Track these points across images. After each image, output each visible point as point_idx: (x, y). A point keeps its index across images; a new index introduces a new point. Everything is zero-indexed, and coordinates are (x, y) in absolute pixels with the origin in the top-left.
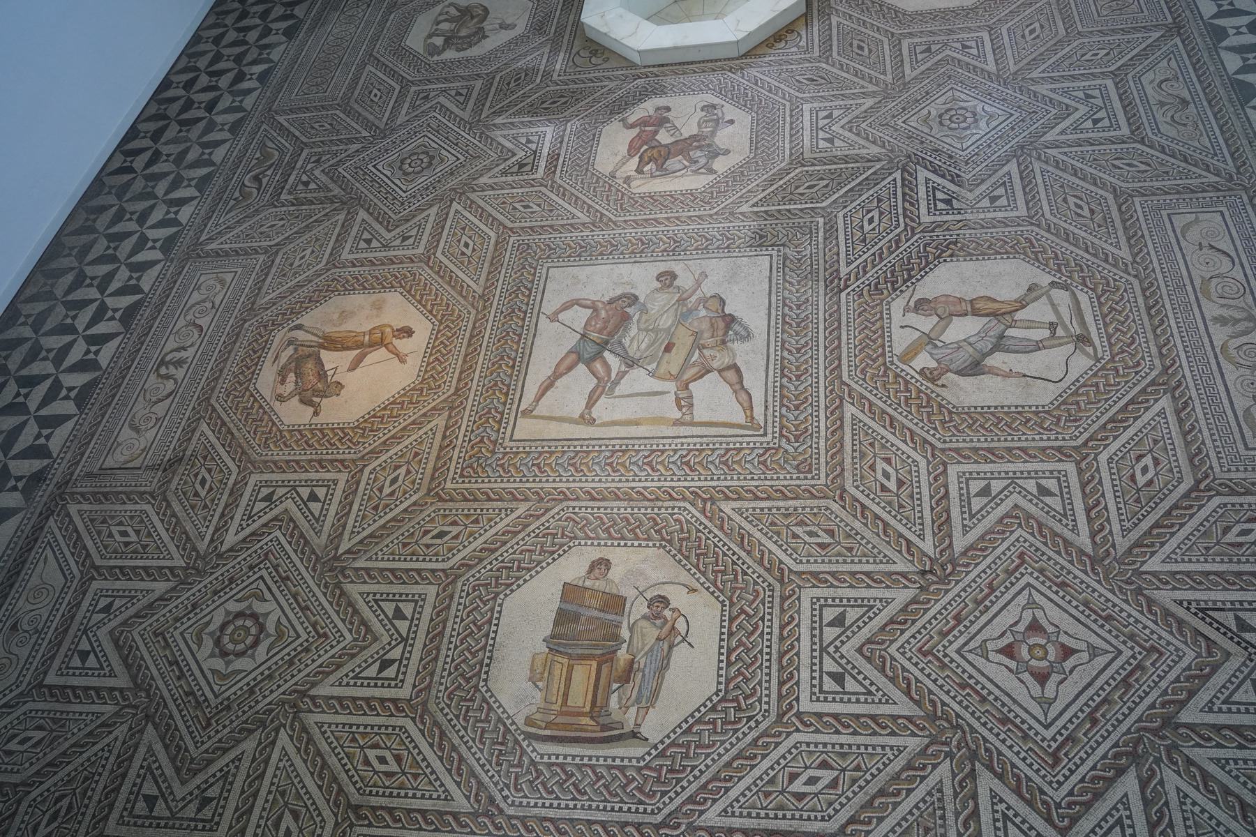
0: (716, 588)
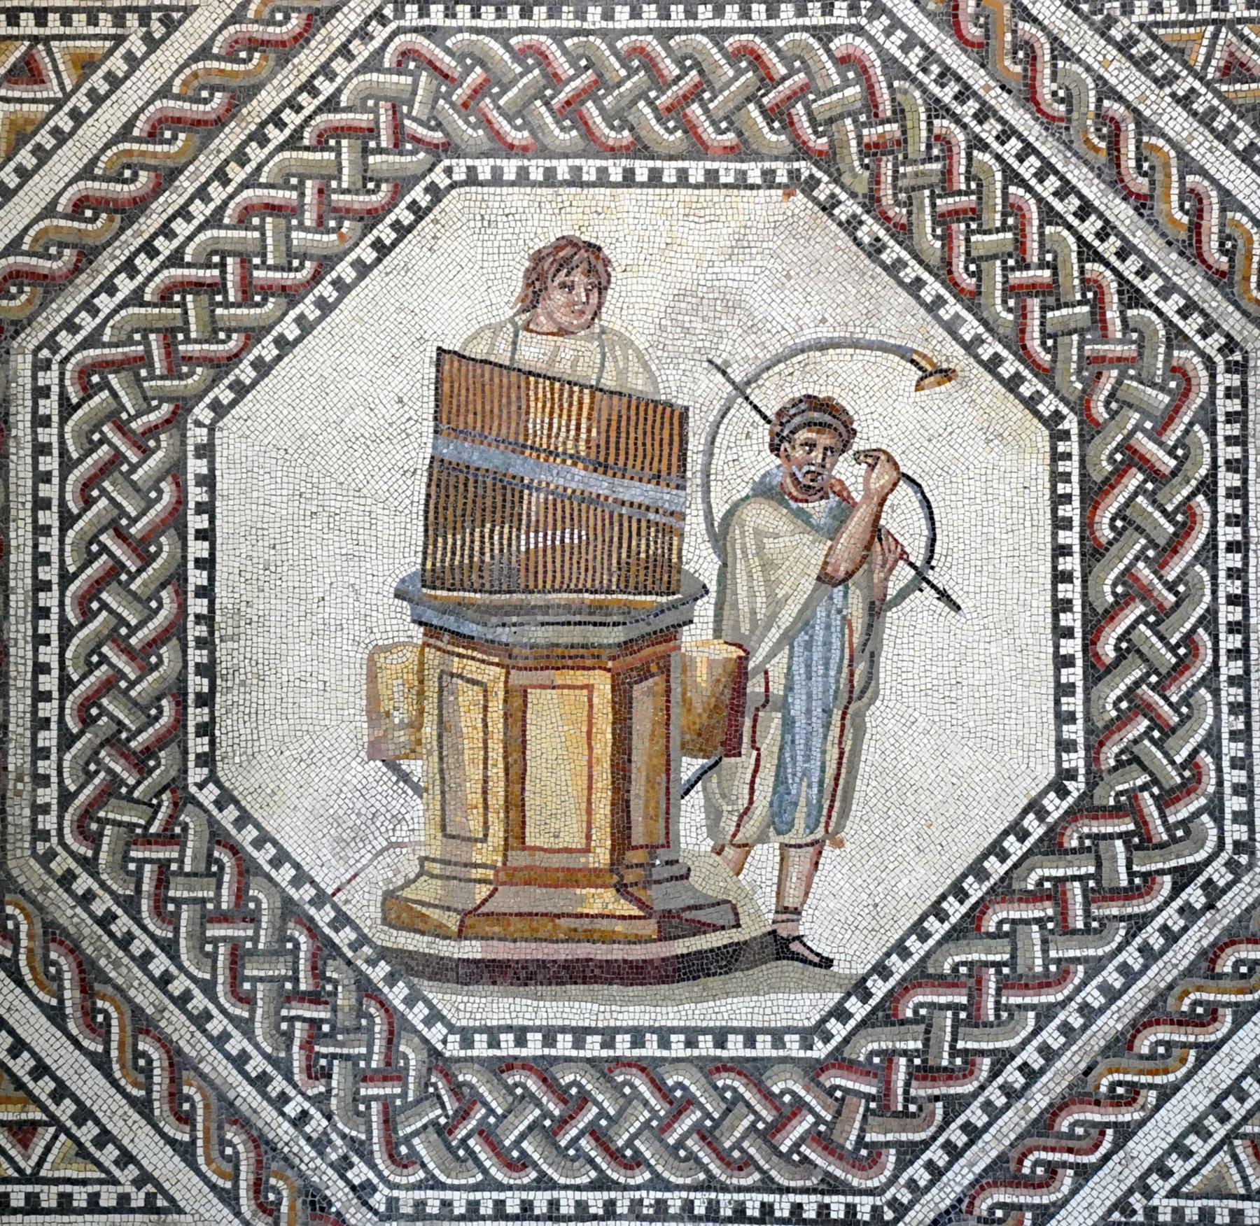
0: (1025, 366)
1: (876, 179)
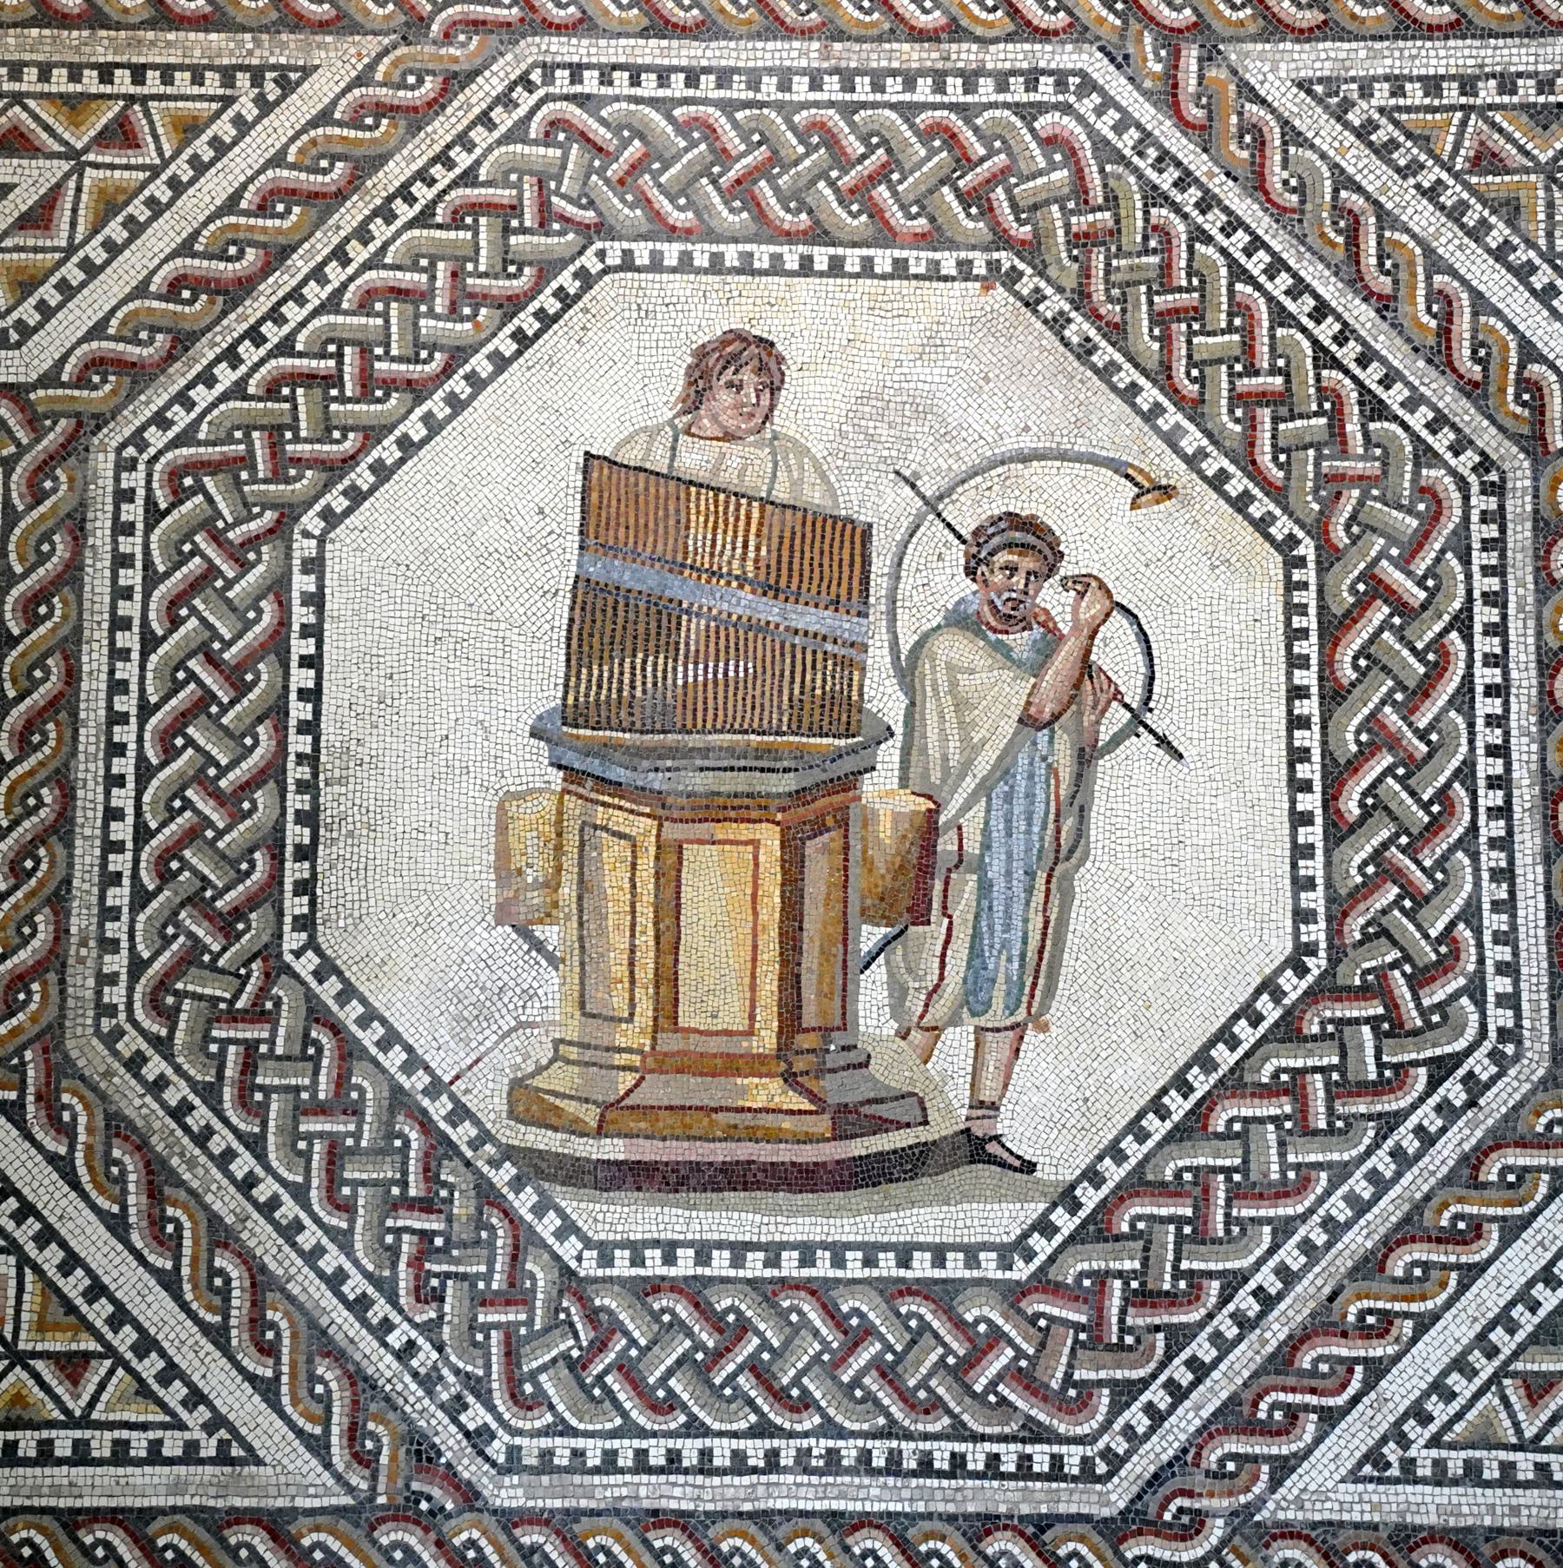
1: (1086, 273)
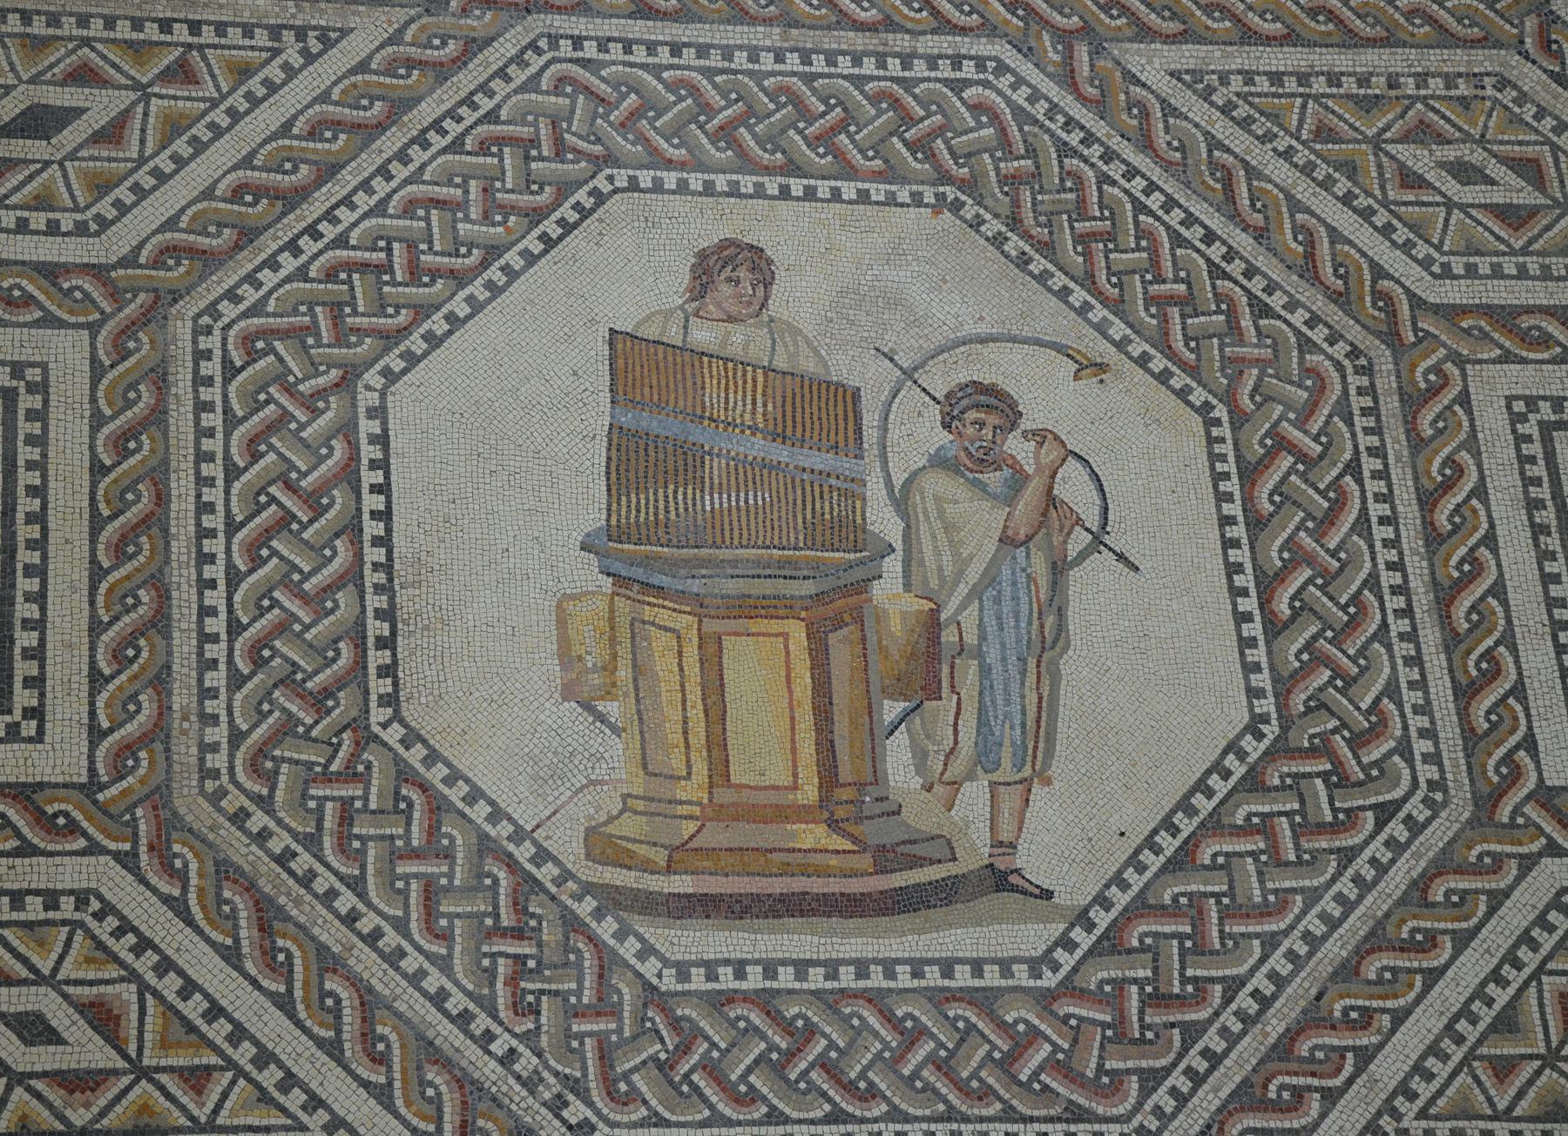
1: (1016, 203)
